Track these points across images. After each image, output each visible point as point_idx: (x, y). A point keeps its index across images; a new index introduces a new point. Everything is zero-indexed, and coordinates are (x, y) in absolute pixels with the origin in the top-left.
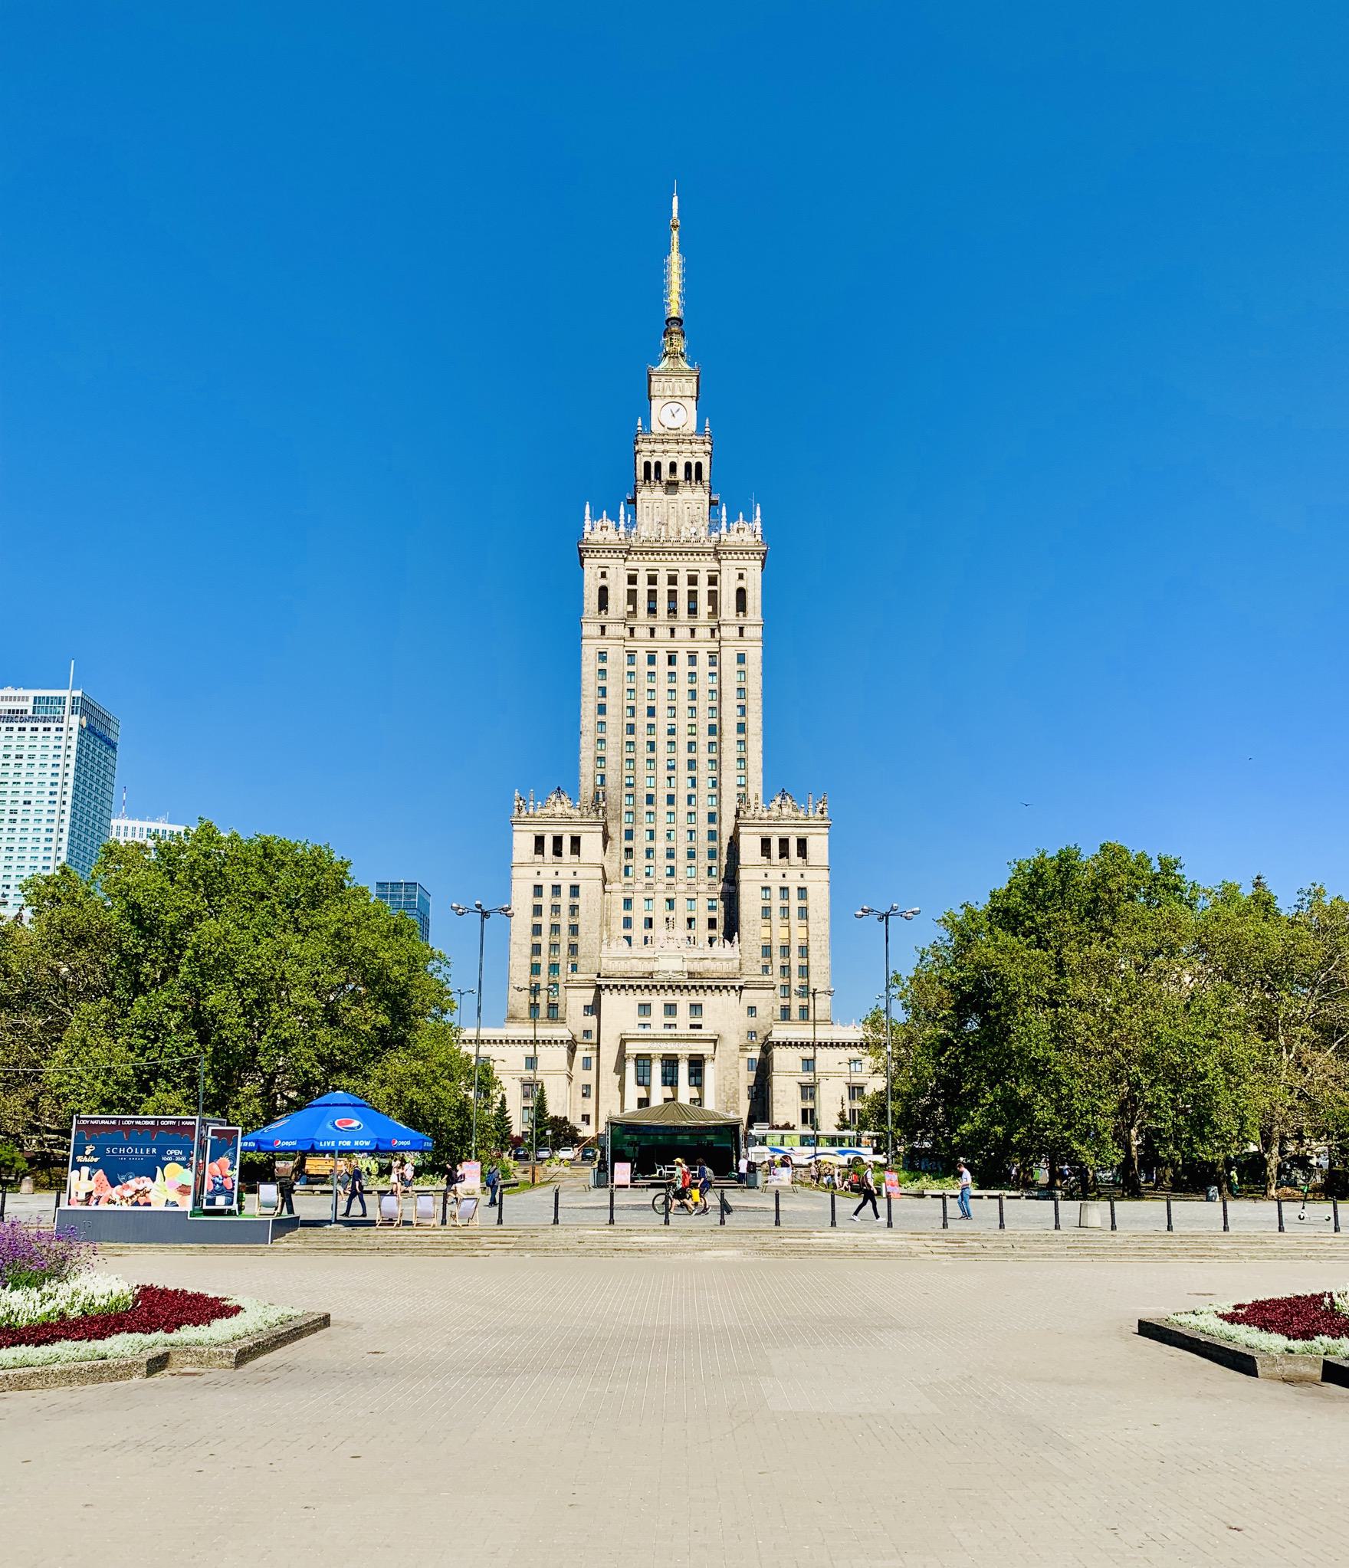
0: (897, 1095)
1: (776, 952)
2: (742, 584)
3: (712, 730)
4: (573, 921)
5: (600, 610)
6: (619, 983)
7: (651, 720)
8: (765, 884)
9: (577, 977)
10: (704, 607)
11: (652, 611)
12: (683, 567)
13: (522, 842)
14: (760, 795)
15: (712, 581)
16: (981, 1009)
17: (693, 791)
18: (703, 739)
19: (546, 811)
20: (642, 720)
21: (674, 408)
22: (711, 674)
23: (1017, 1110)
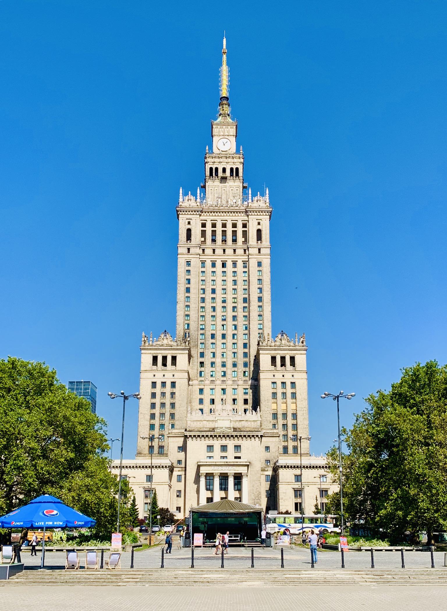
0: (345, 495)
1: (280, 416)
2: (259, 227)
3: (245, 300)
4: (172, 401)
5: (187, 240)
6: (197, 434)
7: (214, 296)
8: (274, 381)
9: (174, 431)
10: (240, 238)
11: (214, 241)
12: (229, 219)
13: (146, 359)
14: (270, 334)
15: (244, 226)
16: (389, 447)
17: (235, 332)
18: (240, 305)
19: (158, 343)
20: (209, 296)
21: (224, 141)
22: (245, 272)
23: (409, 502)
